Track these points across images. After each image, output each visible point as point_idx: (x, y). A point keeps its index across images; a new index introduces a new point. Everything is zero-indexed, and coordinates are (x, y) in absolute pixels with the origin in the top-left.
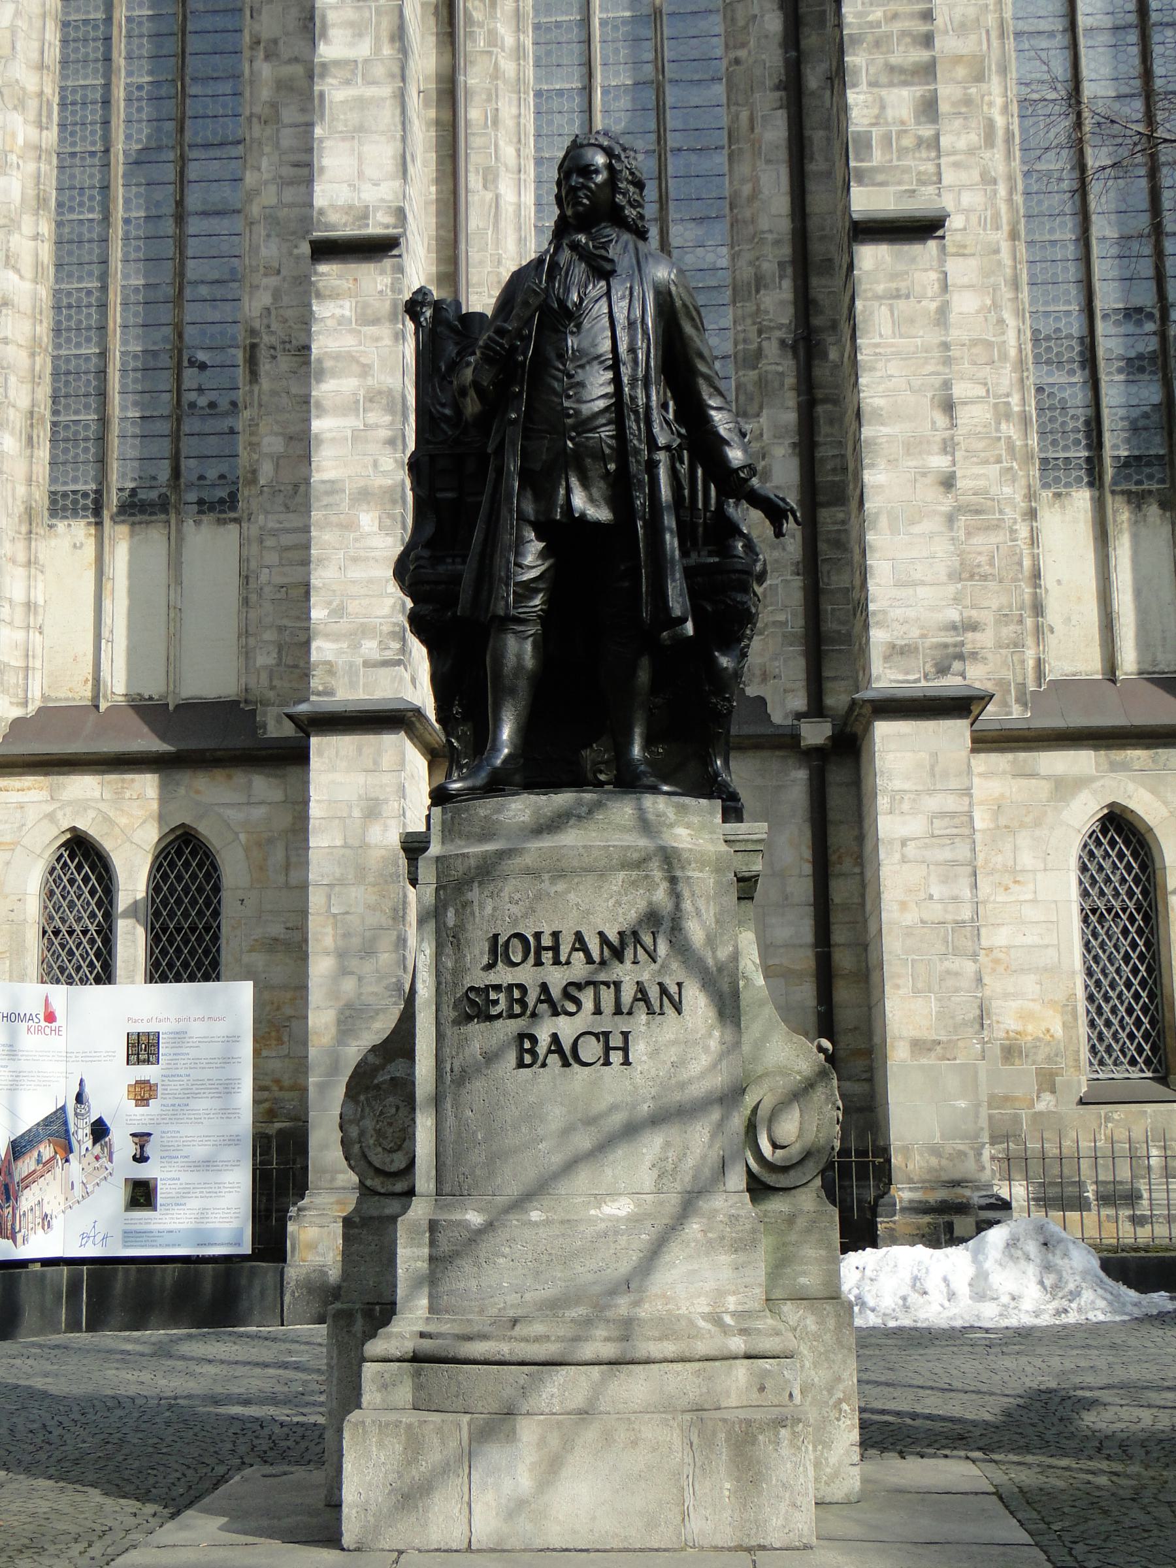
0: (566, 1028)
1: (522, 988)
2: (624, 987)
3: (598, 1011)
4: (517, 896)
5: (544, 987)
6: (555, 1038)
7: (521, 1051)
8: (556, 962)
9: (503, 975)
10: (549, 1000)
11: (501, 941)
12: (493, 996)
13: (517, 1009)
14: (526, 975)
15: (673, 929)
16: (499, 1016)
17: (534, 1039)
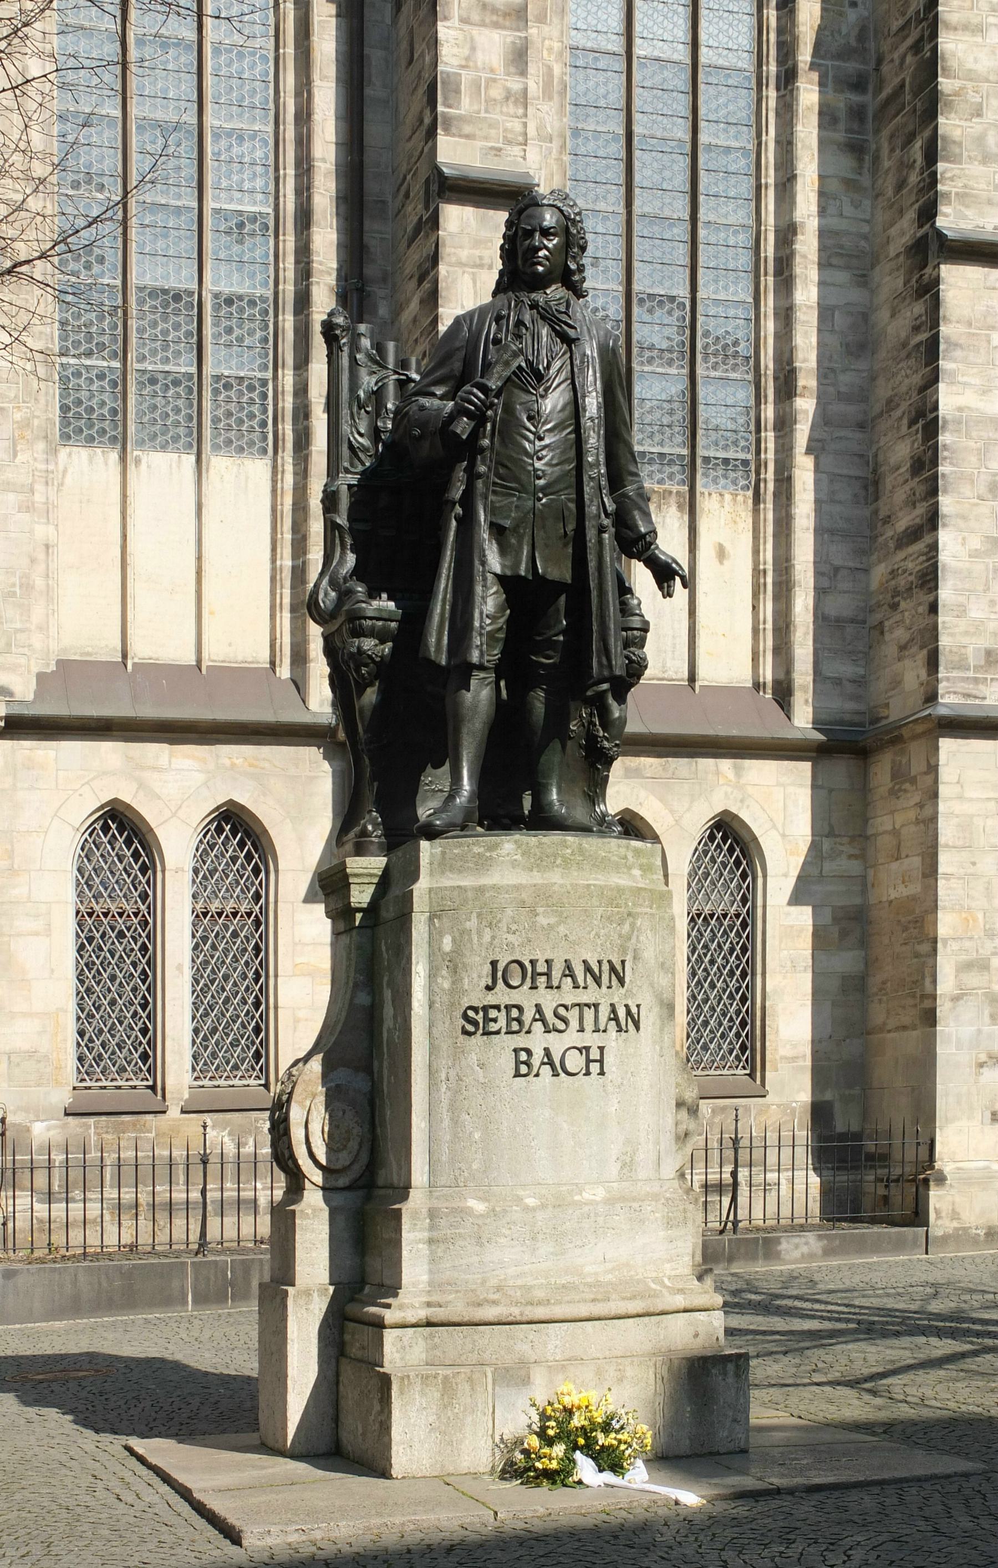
0: (558, 1044)
1: (520, 1008)
2: (601, 1008)
3: (582, 1030)
4: (514, 927)
5: (538, 1008)
6: (547, 1052)
7: (518, 1063)
8: (549, 987)
9: (502, 996)
10: (543, 1020)
11: (501, 967)
12: (493, 1014)
13: (515, 1026)
14: (524, 997)
15: (635, 958)
16: (498, 1032)
17: (528, 1052)
